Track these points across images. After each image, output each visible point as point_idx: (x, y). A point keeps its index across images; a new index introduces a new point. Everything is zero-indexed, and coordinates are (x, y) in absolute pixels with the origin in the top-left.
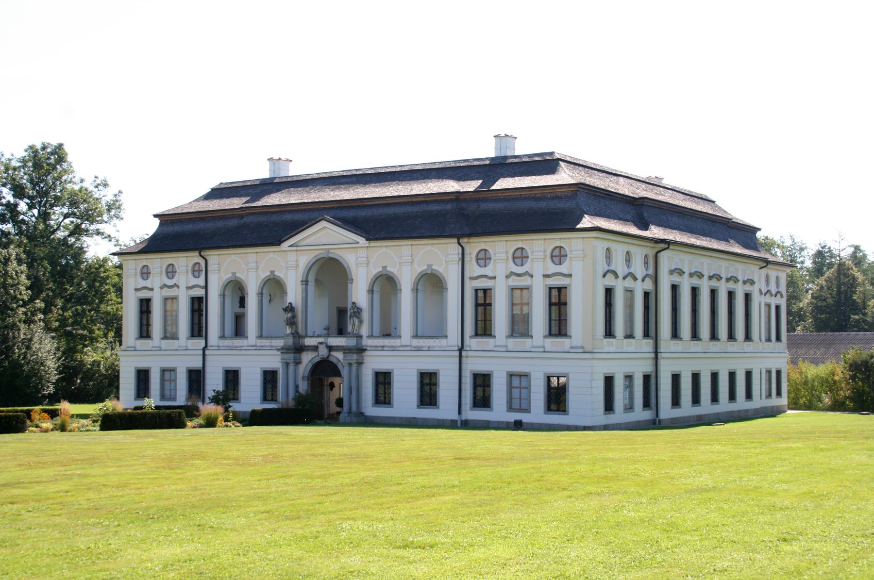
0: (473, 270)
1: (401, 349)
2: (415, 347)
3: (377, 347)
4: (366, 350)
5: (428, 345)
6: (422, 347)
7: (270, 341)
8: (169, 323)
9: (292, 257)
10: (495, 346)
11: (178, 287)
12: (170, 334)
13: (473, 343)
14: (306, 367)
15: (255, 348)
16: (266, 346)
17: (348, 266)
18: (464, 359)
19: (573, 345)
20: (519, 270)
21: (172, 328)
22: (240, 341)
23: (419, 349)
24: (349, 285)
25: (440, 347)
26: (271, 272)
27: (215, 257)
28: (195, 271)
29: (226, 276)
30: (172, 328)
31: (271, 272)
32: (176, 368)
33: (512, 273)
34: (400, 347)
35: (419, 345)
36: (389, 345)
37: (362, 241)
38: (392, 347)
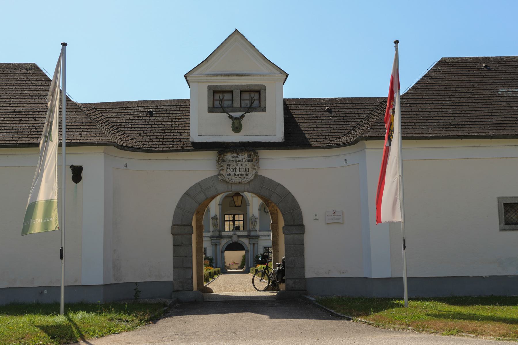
3: (265, 235)
4: (259, 237)
14: (223, 246)
17: (247, 198)
24: (248, 207)
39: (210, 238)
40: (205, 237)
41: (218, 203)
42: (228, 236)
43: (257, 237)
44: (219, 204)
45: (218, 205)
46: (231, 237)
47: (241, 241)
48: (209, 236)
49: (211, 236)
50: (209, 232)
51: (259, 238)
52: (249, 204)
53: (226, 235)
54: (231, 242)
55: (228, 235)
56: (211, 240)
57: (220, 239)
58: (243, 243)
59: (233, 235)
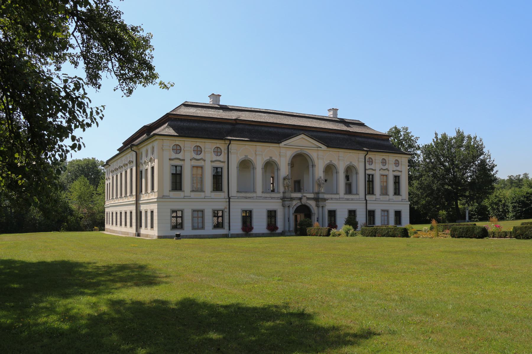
0: (368, 167)
1: (340, 199)
2: (346, 199)
5: (351, 198)
6: (349, 199)
7: (270, 194)
8: (195, 182)
9: (283, 151)
10: (376, 199)
11: (205, 161)
12: (195, 189)
13: (368, 197)
15: (262, 198)
16: (269, 197)
18: (368, 204)
19: (403, 199)
20: (384, 168)
21: (197, 185)
22: (251, 194)
23: (348, 200)
25: (357, 199)
26: (270, 157)
27: (234, 146)
28: (218, 151)
29: (242, 157)
30: (197, 185)
31: (270, 157)
32: (204, 209)
33: (382, 169)
34: (340, 198)
35: (347, 198)
36: (334, 197)
37: (324, 147)
38: (336, 198)
39: (280, 199)
40: (276, 198)
41: (288, 163)
42: (296, 197)
43: (325, 200)
44: (288, 164)
45: (287, 165)
46: (300, 199)
47: (308, 203)
48: (279, 198)
49: (281, 197)
50: (278, 192)
51: (325, 201)
52: (315, 165)
53: (295, 196)
54: (300, 204)
55: (296, 196)
56: (282, 201)
57: (292, 201)
58: (311, 205)
59: (303, 197)
